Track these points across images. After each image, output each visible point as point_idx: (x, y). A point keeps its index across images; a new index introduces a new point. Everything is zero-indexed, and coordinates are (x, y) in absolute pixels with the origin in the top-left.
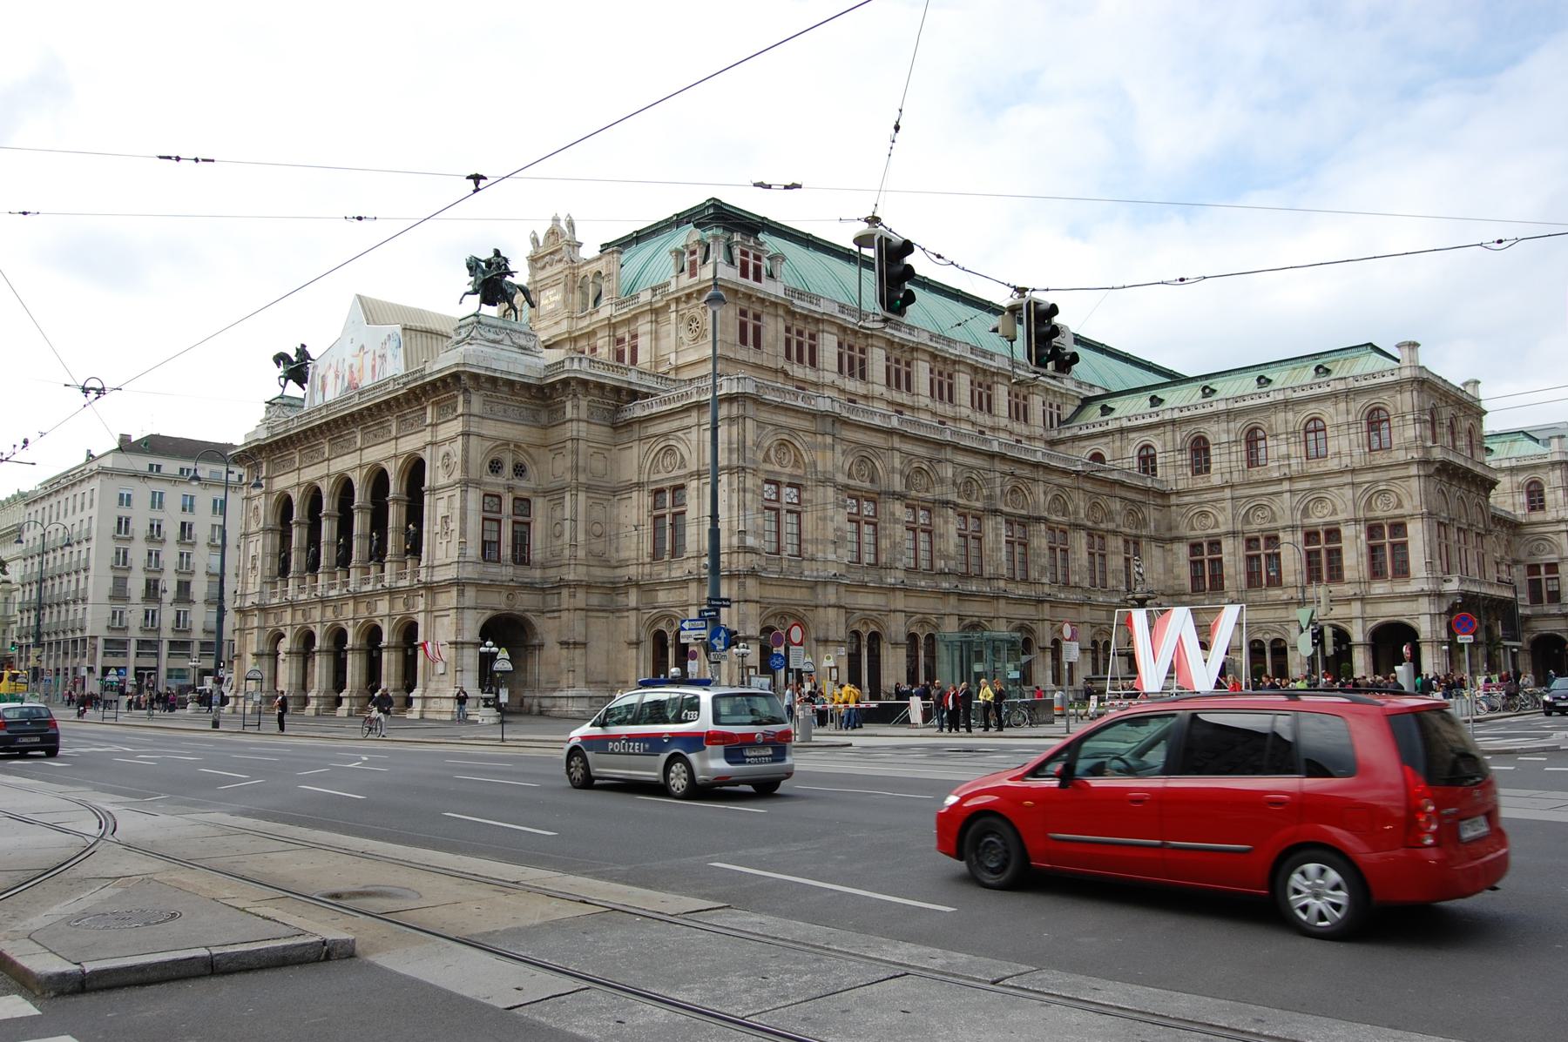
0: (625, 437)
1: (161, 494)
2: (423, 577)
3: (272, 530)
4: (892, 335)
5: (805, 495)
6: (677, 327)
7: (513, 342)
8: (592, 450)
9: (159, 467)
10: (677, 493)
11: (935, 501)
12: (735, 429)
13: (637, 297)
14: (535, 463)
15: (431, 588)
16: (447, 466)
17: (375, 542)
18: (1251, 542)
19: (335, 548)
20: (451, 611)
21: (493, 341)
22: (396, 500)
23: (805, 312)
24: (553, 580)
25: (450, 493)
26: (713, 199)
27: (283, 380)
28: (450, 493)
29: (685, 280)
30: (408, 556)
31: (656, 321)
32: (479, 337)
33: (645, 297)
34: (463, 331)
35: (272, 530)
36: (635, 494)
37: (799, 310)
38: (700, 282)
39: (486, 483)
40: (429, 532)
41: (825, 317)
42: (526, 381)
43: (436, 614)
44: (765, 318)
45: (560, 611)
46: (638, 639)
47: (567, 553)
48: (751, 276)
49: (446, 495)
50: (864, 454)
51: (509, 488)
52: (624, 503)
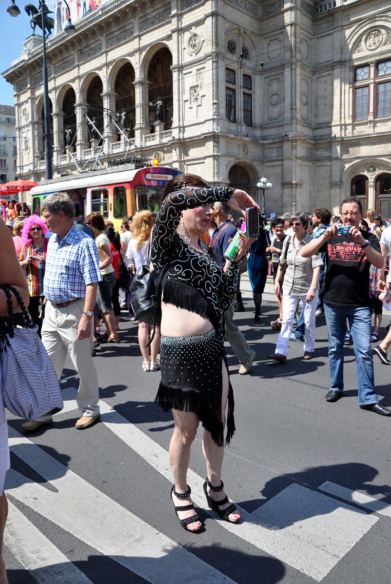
0: (324, 26)
2: (175, 133)
8: (302, 36)
10: (381, 66)
14: (255, 49)
15: (184, 145)
17: (124, 117)
19: (86, 127)
20: (207, 159)
22: (141, 83)
24: (272, 137)
27: (33, 24)
30: (157, 122)
35: (37, 123)
36: (337, 71)
39: (227, 59)
40: (179, 100)
43: (187, 163)
45: (282, 160)
46: (341, 181)
47: (288, 115)
49: (194, 70)
51: (240, 65)
52: (323, 80)
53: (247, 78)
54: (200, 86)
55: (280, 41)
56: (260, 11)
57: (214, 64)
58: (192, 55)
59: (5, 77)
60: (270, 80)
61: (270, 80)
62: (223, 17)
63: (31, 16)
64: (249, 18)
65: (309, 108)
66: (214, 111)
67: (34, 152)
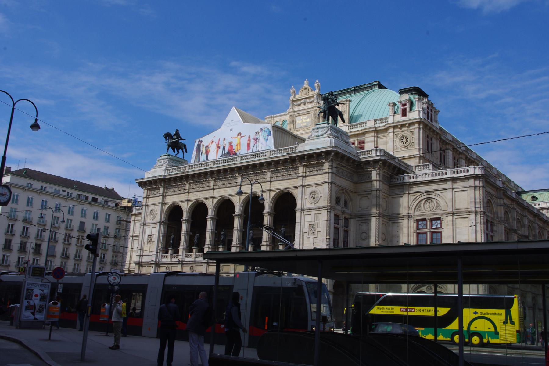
1: (32, 199)
5: (495, 228)
6: (393, 140)
7: (342, 139)
9: (31, 184)
10: (434, 222)
11: (523, 235)
12: (477, 192)
13: (366, 123)
16: (314, 198)
17: (251, 234)
22: (270, 214)
23: (444, 139)
25: (316, 212)
26: (378, 81)
27: (168, 146)
28: (316, 212)
29: (399, 118)
31: (377, 137)
33: (370, 124)
34: (320, 130)
35: (164, 223)
37: (443, 138)
38: (410, 120)
41: (450, 142)
42: (355, 158)
44: (434, 140)
49: (313, 213)
50: (507, 210)
53: (346, 219)
54: (317, 224)
55: (369, 198)
57: (329, 213)
58: (312, 204)
59: (137, 183)
60: (361, 223)
61: (361, 223)
62: (334, 184)
63: (168, 140)
64: (349, 182)
65: (387, 242)
66: (327, 243)
67: (158, 247)
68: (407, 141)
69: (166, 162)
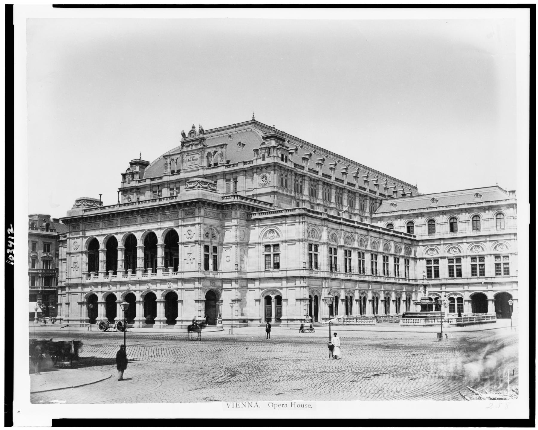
3: (85, 252)
4: (325, 180)
18: (451, 260)
21: (206, 188)
31: (246, 175)
32: (200, 186)
35: (85, 252)
36: (257, 246)
44: (289, 177)
48: (285, 161)
49: (190, 246)
56: (221, 216)
68: (266, 180)
69: (83, 203)
